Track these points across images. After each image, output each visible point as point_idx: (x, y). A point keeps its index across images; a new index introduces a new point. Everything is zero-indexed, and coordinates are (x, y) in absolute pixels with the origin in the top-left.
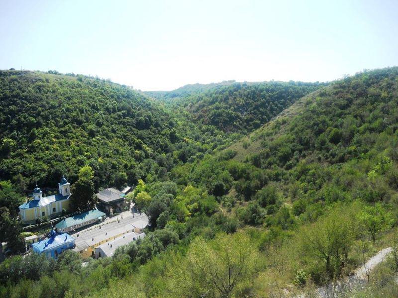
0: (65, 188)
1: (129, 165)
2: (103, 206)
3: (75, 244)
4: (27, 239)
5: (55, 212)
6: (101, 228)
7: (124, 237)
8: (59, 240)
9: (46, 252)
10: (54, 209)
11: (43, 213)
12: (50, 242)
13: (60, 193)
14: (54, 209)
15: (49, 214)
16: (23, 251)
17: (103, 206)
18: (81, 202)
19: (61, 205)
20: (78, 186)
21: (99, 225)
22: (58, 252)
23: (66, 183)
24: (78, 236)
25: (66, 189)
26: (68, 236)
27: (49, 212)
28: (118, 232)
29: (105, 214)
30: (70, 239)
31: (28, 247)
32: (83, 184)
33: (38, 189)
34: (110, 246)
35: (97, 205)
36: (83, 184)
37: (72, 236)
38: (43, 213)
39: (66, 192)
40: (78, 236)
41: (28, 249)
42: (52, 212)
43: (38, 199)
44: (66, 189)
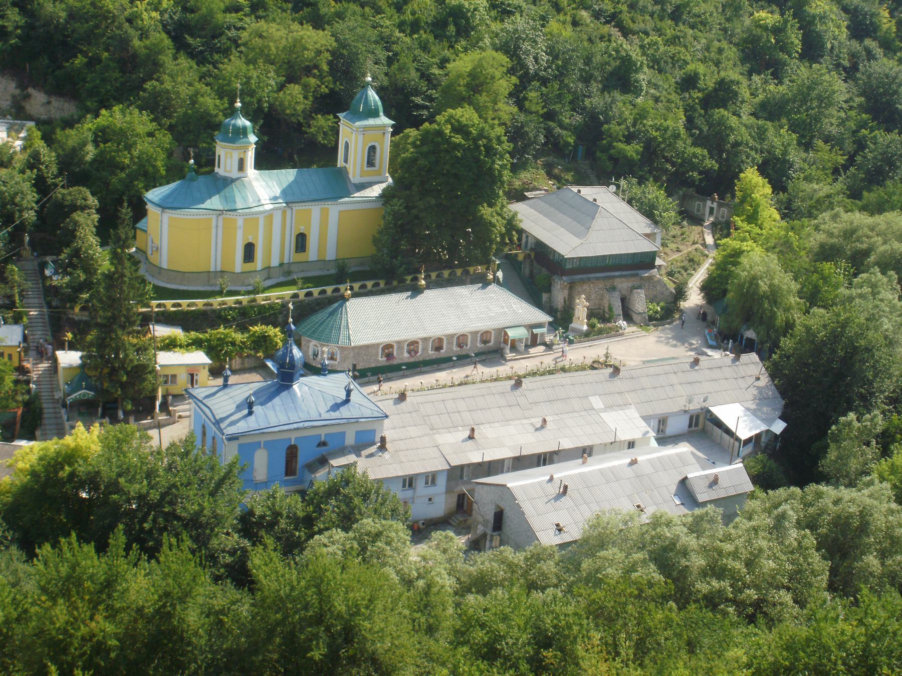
0: (364, 138)
1: (708, 82)
2: (537, 273)
3: (383, 440)
4: (164, 358)
5: (301, 257)
6: (518, 384)
7: (634, 462)
8: (313, 399)
9: (247, 444)
10: (301, 242)
11: (249, 252)
12: (266, 396)
13: (340, 163)
14: (301, 242)
15: (275, 262)
16: (144, 407)
17: (537, 273)
18: (435, 225)
19: (335, 225)
20: (434, 144)
21: (503, 370)
22: (296, 458)
23: (374, 114)
24: (402, 397)
25: (372, 149)
26: (354, 386)
27: (274, 251)
28: (583, 426)
29: (545, 318)
30: (367, 400)
31: (165, 397)
32: (458, 139)
33: (243, 122)
34: (554, 490)
35: (511, 263)
36: (458, 139)
37: (367, 390)
38: (249, 252)
39: (371, 163)
40: (402, 397)
41: (164, 407)
42: (290, 256)
43: (234, 173)
44: (372, 149)
